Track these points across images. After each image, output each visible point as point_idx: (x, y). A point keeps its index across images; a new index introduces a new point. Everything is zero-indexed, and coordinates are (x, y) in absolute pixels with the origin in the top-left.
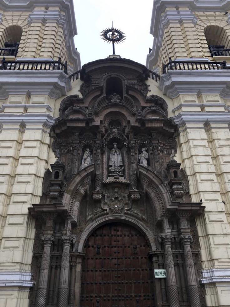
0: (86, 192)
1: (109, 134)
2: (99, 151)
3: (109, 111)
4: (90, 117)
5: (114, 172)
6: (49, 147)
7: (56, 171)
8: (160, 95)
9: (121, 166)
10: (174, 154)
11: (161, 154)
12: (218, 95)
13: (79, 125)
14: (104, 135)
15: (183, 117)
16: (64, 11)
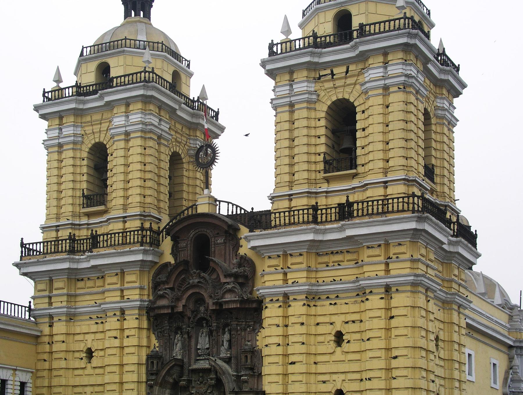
0: (174, 379)
1: (196, 316)
2: (186, 336)
3: (190, 292)
4: (173, 304)
5: (202, 355)
6: (148, 329)
7: (151, 360)
8: (250, 254)
9: (208, 349)
10: (259, 329)
11: (243, 333)
12: (305, 254)
13: (166, 311)
14: (191, 318)
15: (261, 291)
16: (150, 103)
